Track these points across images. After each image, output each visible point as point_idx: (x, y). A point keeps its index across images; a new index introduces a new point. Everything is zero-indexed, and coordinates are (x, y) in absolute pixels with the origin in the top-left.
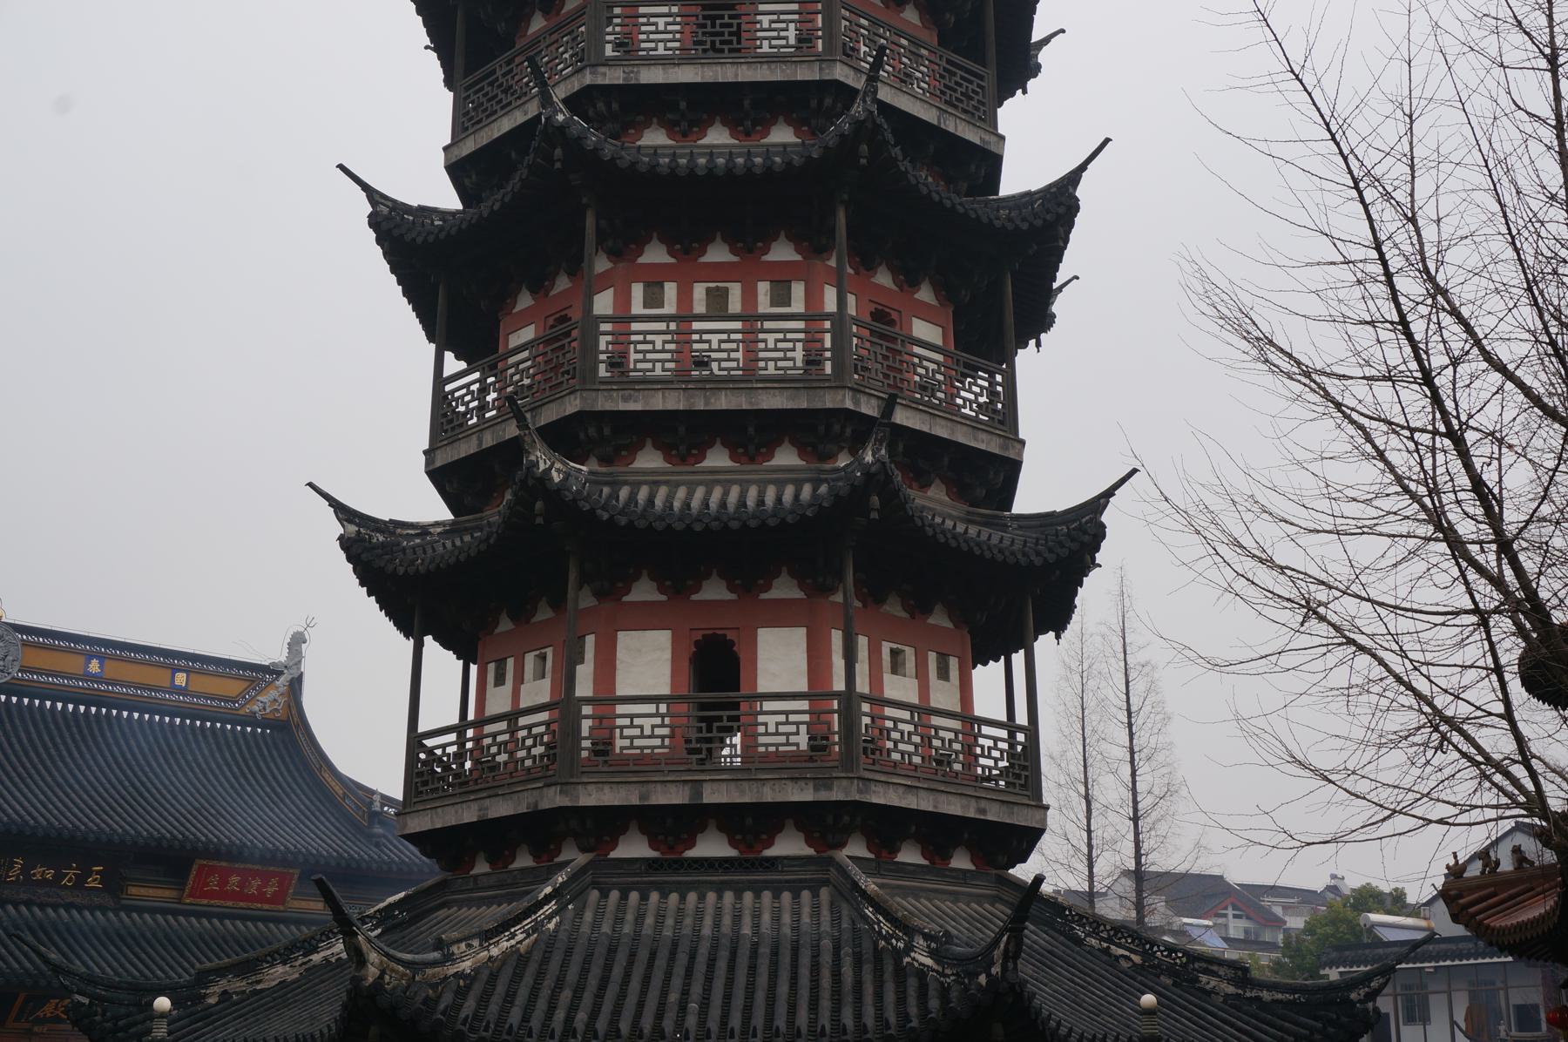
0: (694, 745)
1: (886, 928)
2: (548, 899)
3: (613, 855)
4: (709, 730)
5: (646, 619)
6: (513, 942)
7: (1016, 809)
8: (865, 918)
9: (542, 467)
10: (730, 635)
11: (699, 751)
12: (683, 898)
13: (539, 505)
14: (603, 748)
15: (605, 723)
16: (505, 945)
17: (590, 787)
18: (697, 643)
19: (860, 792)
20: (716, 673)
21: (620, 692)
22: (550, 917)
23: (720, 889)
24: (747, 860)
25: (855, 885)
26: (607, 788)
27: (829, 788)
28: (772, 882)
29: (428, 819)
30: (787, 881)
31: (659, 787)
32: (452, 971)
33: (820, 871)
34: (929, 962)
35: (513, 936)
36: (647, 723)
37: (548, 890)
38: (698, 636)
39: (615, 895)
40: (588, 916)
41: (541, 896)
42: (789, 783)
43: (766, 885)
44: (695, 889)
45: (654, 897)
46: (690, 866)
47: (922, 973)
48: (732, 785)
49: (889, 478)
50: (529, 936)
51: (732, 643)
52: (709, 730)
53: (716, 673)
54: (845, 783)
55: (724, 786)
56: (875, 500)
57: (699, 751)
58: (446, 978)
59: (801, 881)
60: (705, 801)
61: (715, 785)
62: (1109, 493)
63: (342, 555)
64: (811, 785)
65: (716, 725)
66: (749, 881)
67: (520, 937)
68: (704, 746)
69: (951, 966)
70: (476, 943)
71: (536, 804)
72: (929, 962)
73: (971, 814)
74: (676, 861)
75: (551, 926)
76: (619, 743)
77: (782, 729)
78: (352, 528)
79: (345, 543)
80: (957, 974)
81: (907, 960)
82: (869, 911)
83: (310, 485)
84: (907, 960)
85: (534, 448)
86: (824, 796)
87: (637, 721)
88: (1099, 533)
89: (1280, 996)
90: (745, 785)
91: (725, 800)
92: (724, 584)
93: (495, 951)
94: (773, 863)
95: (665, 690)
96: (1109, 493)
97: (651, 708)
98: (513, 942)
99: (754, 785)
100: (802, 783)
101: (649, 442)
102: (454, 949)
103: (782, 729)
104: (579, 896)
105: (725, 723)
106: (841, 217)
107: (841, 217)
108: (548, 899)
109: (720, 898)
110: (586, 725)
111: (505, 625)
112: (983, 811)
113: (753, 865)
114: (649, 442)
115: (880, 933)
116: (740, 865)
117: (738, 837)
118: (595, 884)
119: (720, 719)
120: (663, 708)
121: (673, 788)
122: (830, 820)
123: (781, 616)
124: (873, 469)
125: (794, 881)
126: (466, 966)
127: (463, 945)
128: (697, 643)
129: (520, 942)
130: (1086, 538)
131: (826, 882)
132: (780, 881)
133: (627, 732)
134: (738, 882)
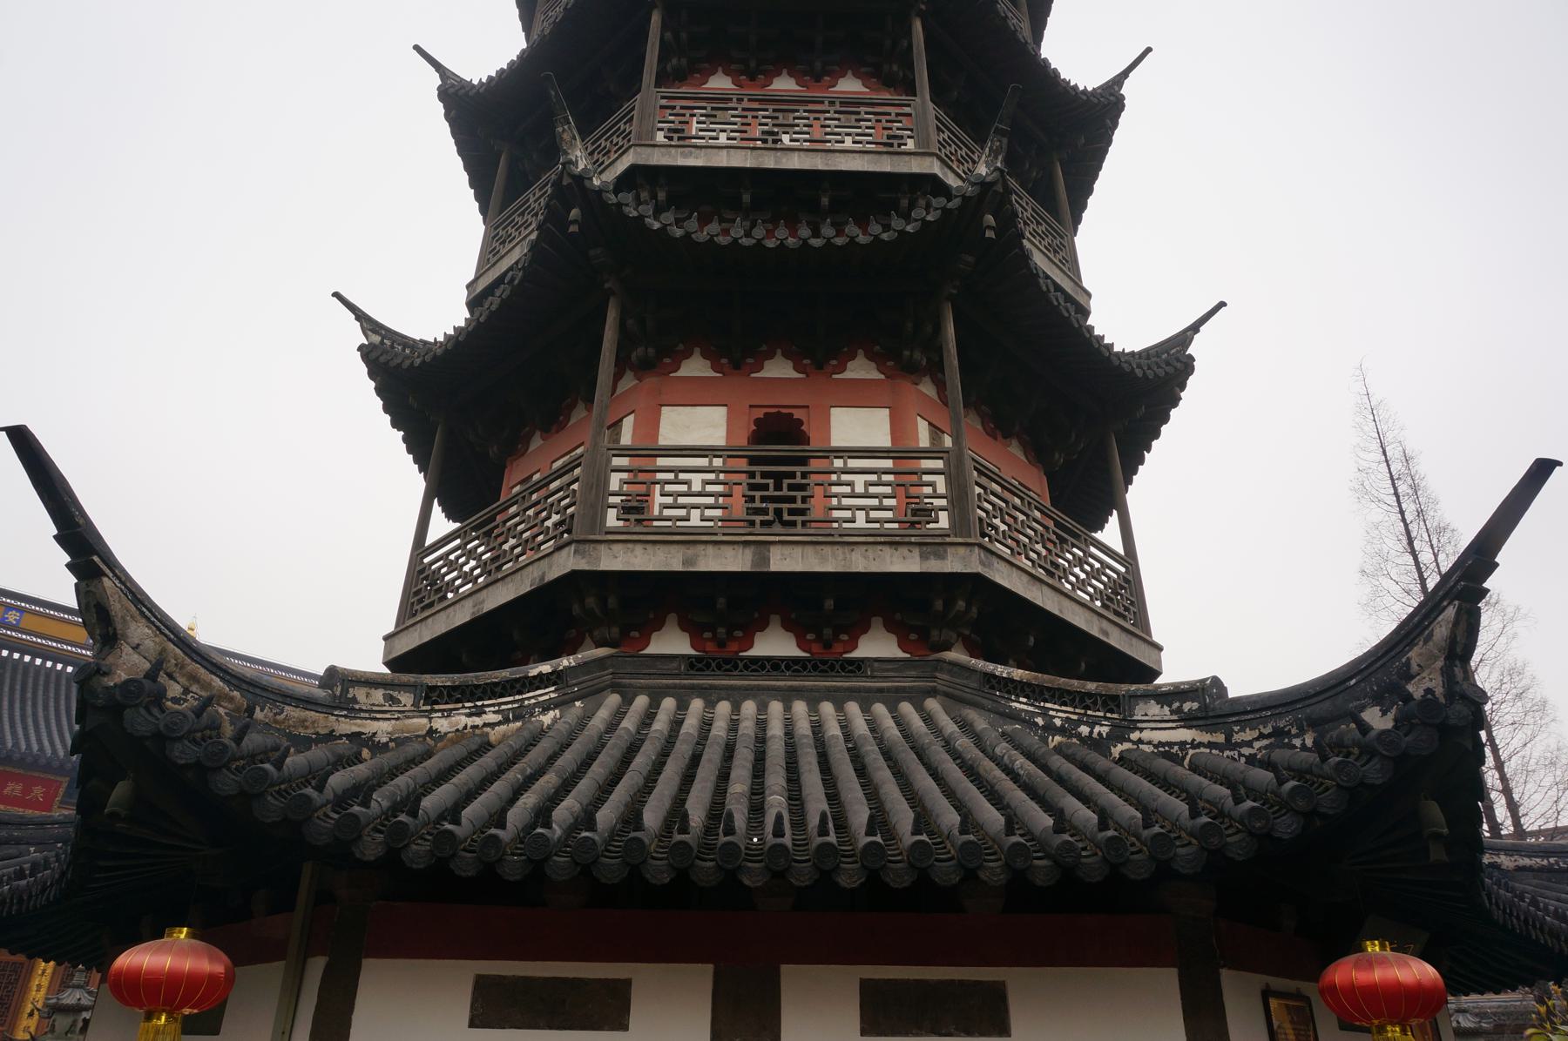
0: (758, 504)
1: (1059, 714)
2: (542, 681)
3: (646, 652)
4: (778, 487)
5: (697, 394)
6: (478, 721)
7: (1134, 640)
8: (1014, 716)
9: (581, 166)
10: (797, 414)
11: (765, 511)
12: (736, 708)
13: (575, 213)
14: (635, 509)
15: (643, 478)
16: (462, 720)
17: (616, 547)
18: (757, 422)
19: (982, 563)
20: (779, 456)
21: (663, 441)
22: (546, 708)
23: (787, 697)
24: (824, 662)
25: (990, 678)
26: (639, 548)
27: (942, 557)
28: (858, 690)
29: (416, 634)
30: (881, 690)
31: (710, 549)
32: (346, 726)
33: (919, 677)
34: (1185, 735)
35: (479, 712)
36: (697, 481)
37: (546, 668)
38: (760, 413)
39: (641, 701)
40: (603, 714)
41: (534, 672)
42: (887, 549)
43: (852, 694)
44: (754, 697)
45: (697, 705)
46: (746, 667)
47: (1168, 752)
48: (809, 550)
49: (1008, 191)
50: (506, 721)
51: (800, 422)
52: (778, 487)
53: (779, 456)
54: (962, 550)
55: (798, 550)
56: (990, 219)
57: (765, 511)
58: (331, 736)
59: (897, 690)
60: (774, 568)
61: (787, 550)
62: (1195, 328)
63: (363, 369)
64: (916, 551)
65: (786, 482)
66: (828, 689)
67: (491, 717)
68: (772, 506)
69: (1244, 725)
70: (406, 699)
71: (542, 578)
72: (1185, 735)
73: (1095, 632)
74: (727, 661)
75: (547, 719)
76: (659, 500)
77: (872, 490)
78: (376, 339)
79: (366, 353)
80: (1278, 733)
81: (1117, 750)
82: (1021, 705)
83: (336, 295)
84: (1117, 750)
85: (572, 146)
86: (934, 566)
87: (682, 476)
88: (1188, 366)
89: (1526, 862)
90: (827, 550)
91: (799, 568)
92: (790, 364)
93: (442, 725)
94: (859, 666)
95: (722, 442)
96: (1195, 328)
97: (702, 462)
98: (478, 721)
99: (839, 550)
100: (904, 550)
101: (697, 350)
102: (360, 693)
103: (872, 490)
104: (593, 694)
105: (798, 480)
106: (918, 26)
107: (918, 26)
108: (542, 681)
109: (788, 709)
110: (615, 481)
111: (536, 442)
112: (1106, 634)
113: (832, 668)
114: (697, 350)
115: (1050, 728)
116: (815, 667)
117: (809, 637)
118: (615, 687)
119: (792, 475)
120: (718, 462)
121: (728, 551)
122: (939, 605)
123: (859, 396)
124: (989, 179)
125: (889, 690)
126: (382, 729)
127: (378, 695)
128: (757, 422)
129: (492, 725)
130: (1179, 365)
131: (932, 693)
132: (869, 690)
133: (668, 488)
134: (811, 690)
